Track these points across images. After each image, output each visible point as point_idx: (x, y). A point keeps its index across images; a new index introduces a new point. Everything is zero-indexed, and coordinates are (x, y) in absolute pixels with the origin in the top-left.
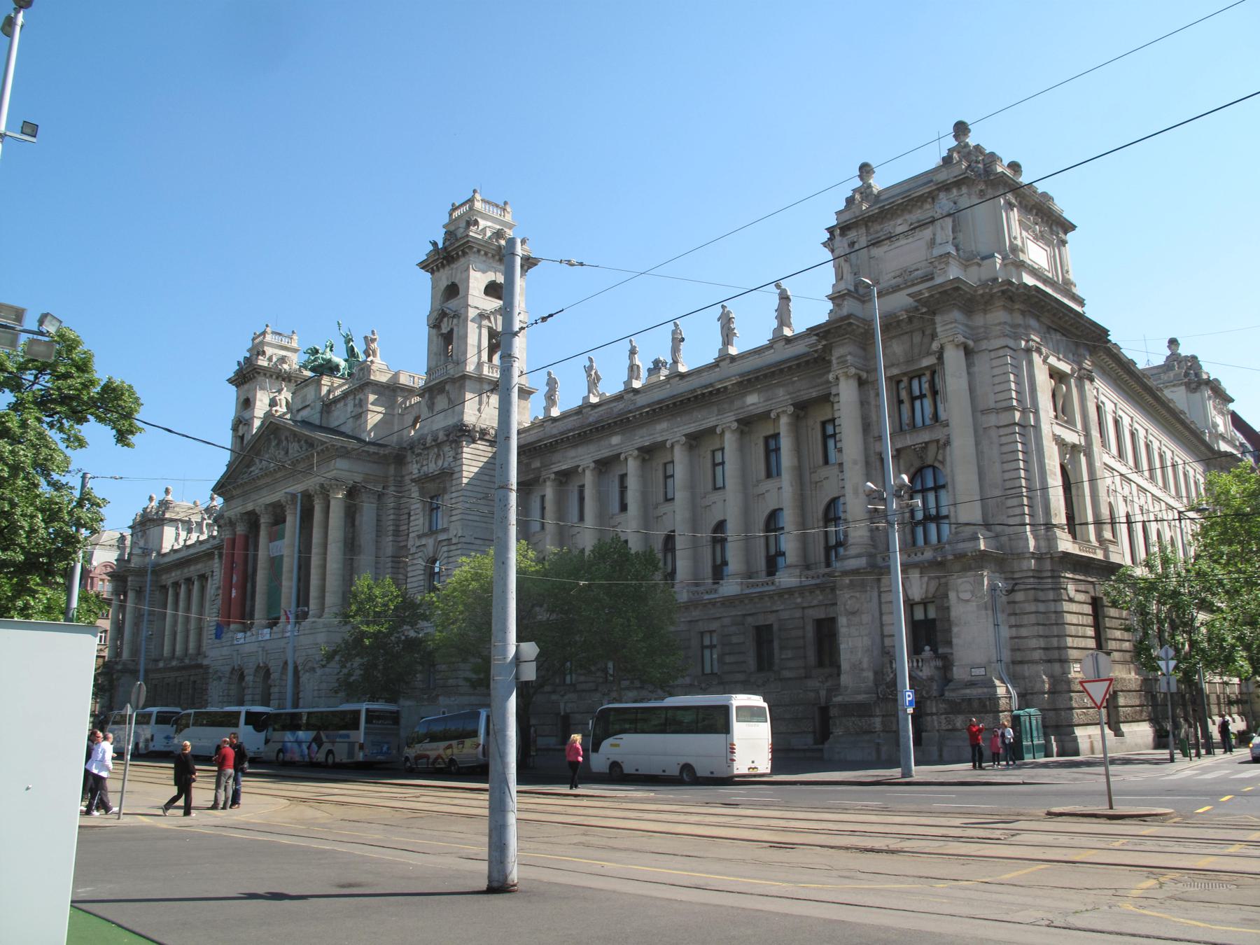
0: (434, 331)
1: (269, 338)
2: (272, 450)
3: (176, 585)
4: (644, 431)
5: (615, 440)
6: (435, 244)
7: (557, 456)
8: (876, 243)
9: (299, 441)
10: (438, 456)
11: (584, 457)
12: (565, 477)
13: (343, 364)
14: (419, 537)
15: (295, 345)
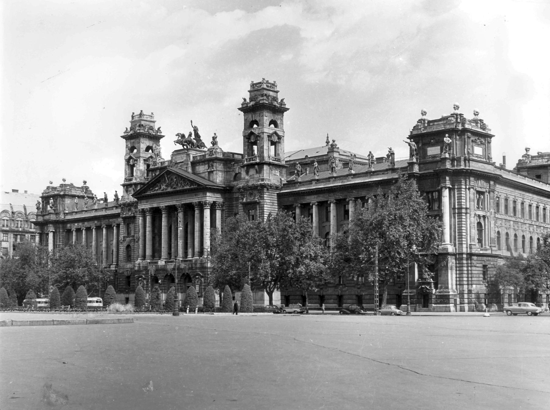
0: (246, 140)
3: (79, 230)
6: (245, 100)
9: (184, 181)
13: (195, 141)
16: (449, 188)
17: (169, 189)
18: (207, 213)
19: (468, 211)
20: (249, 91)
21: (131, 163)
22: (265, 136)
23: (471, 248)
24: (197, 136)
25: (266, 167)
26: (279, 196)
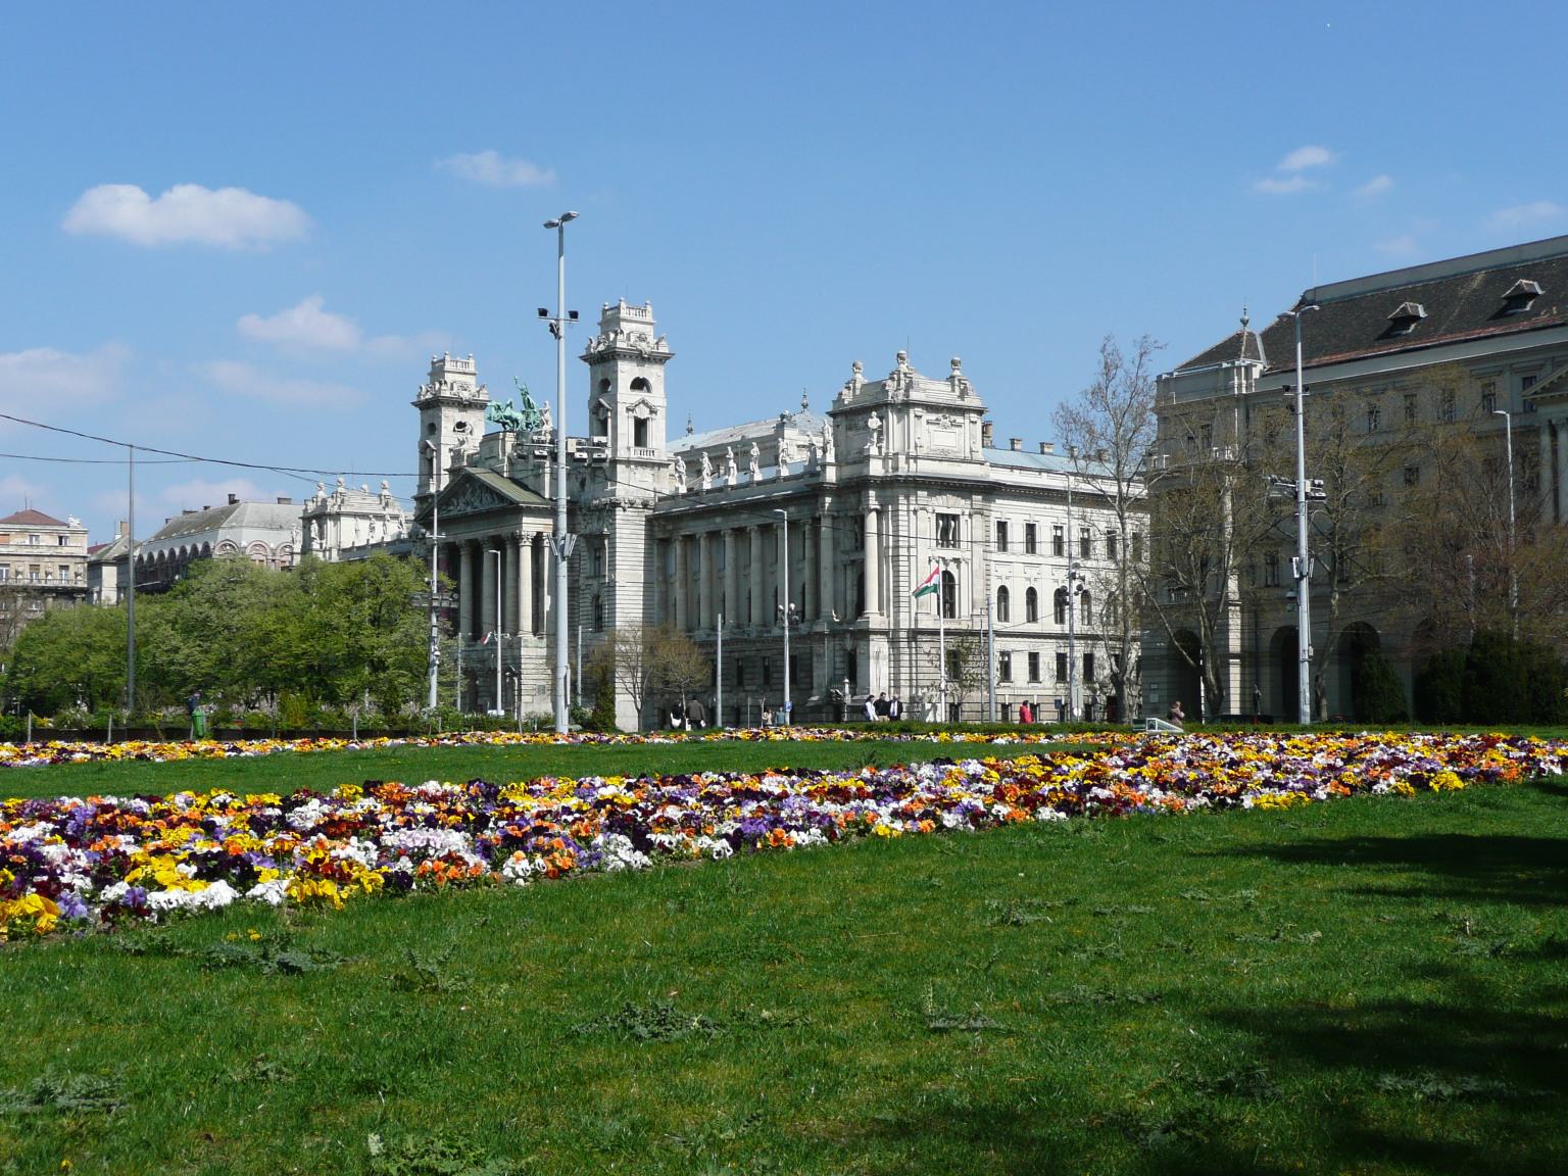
1: (448, 367)
2: (468, 496)
4: (734, 517)
5: (718, 520)
7: (683, 524)
8: (849, 428)
10: (599, 519)
11: (700, 528)
12: (690, 539)
14: (587, 578)
15: (472, 369)
16: (876, 510)
17: (469, 509)
18: (526, 553)
19: (913, 551)
20: (599, 324)
21: (427, 456)
22: (621, 409)
23: (916, 620)
24: (528, 404)
25: (620, 468)
26: (650, 521)
